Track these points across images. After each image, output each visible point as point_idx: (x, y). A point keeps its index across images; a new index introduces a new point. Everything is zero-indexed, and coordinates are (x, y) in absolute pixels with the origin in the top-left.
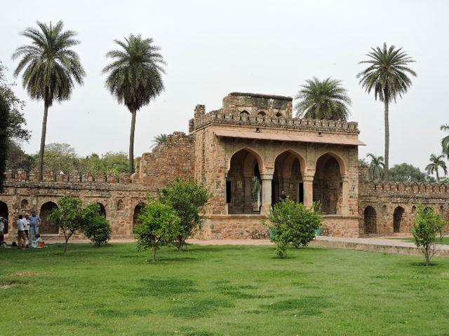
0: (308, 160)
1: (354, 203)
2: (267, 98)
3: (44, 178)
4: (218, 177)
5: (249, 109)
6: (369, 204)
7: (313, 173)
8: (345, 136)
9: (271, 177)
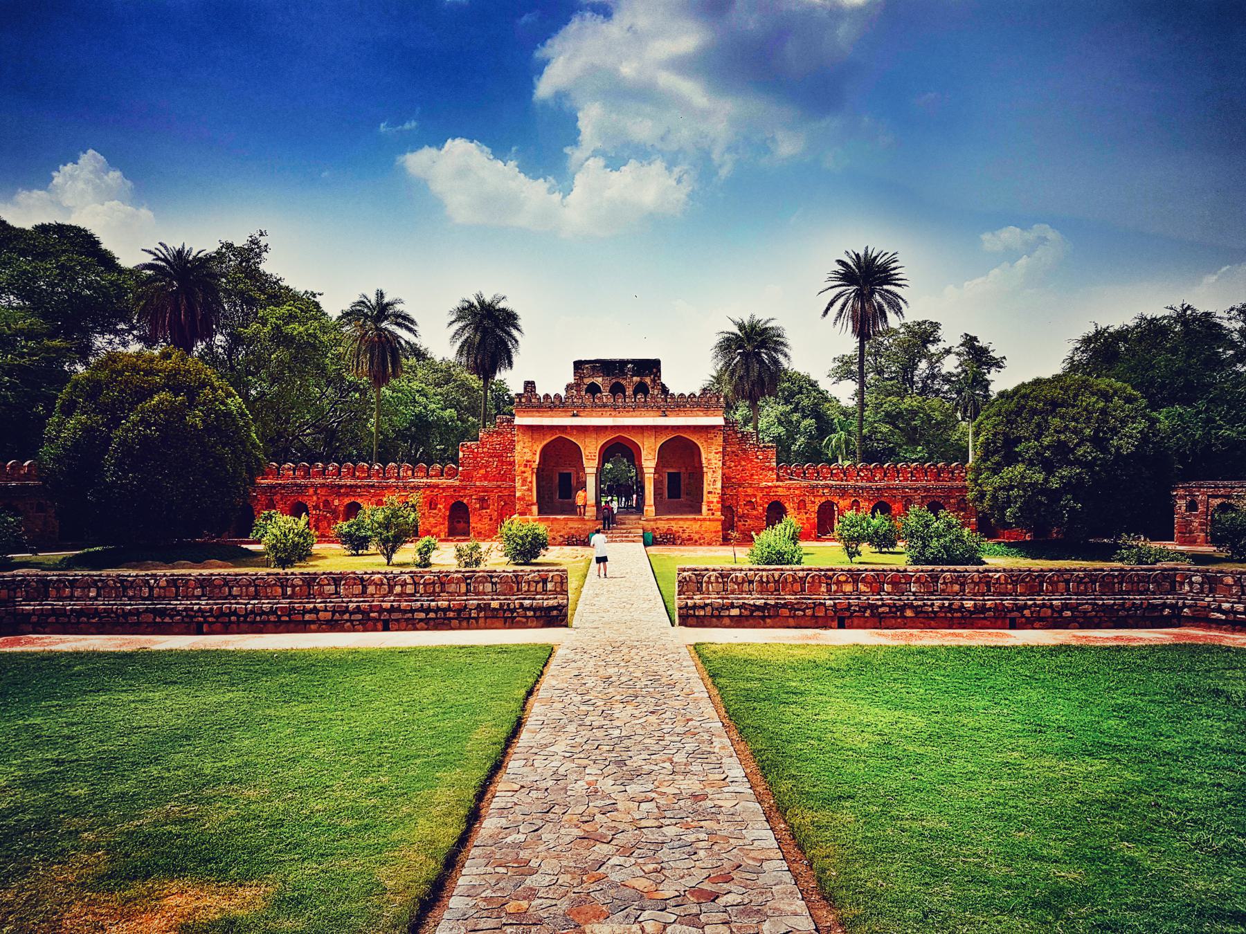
0: (645, 447)
1: (715, 500)
2: (623, 363)
3: (357, 474)
4: (524, 472)
5: (599, 380)
6: (776, 498)
7: (653, 464)
8: (701, 414)
9: (594, 470)
